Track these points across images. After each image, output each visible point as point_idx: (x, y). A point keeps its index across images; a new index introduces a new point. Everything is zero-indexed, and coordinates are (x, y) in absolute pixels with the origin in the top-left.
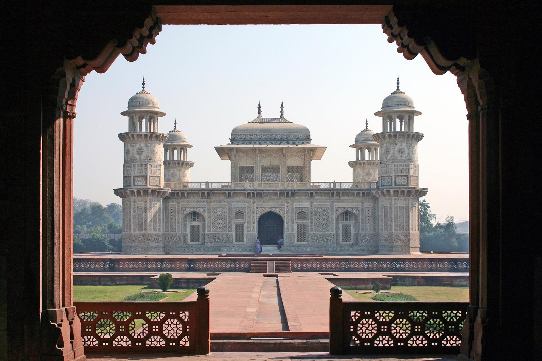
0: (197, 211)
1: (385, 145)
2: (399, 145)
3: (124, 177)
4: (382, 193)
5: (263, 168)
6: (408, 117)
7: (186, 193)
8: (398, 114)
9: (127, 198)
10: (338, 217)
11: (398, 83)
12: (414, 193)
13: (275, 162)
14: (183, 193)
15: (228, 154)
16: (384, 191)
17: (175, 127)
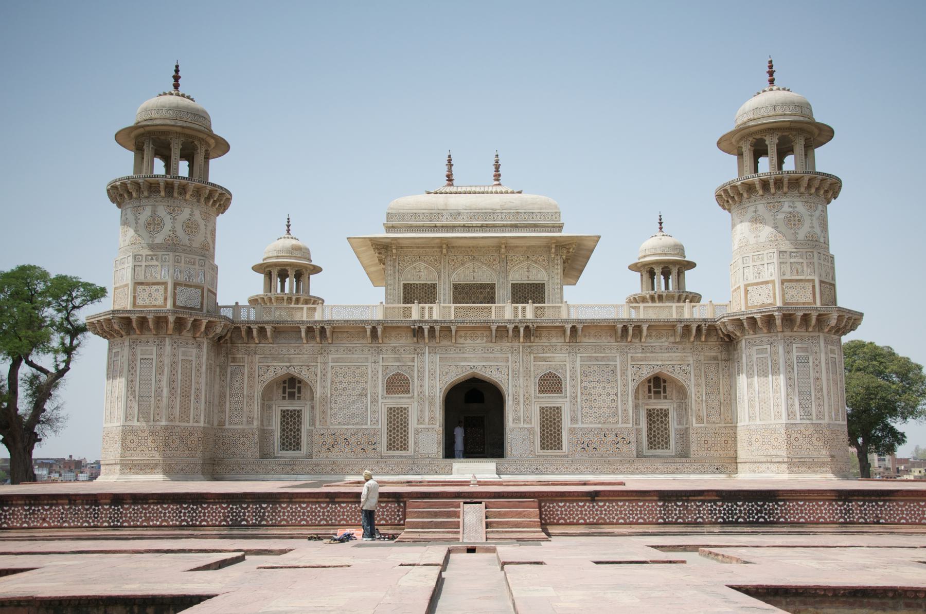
0: (294, 372)
1: (753, 209)
2: (786, 208)
3: (116, 288)
4: (752, 321)
5: (456, 287)
6: (803, 143)
7: (269, 328)
8: (780, 134)
9: (118, 340)
10: (637, 392)
11: (771, 73)
12: (833, 322)
13: (484, 275)
14: (262, 330)
15: (380, 261)
16: (757, 316)
17: (288, 231)
